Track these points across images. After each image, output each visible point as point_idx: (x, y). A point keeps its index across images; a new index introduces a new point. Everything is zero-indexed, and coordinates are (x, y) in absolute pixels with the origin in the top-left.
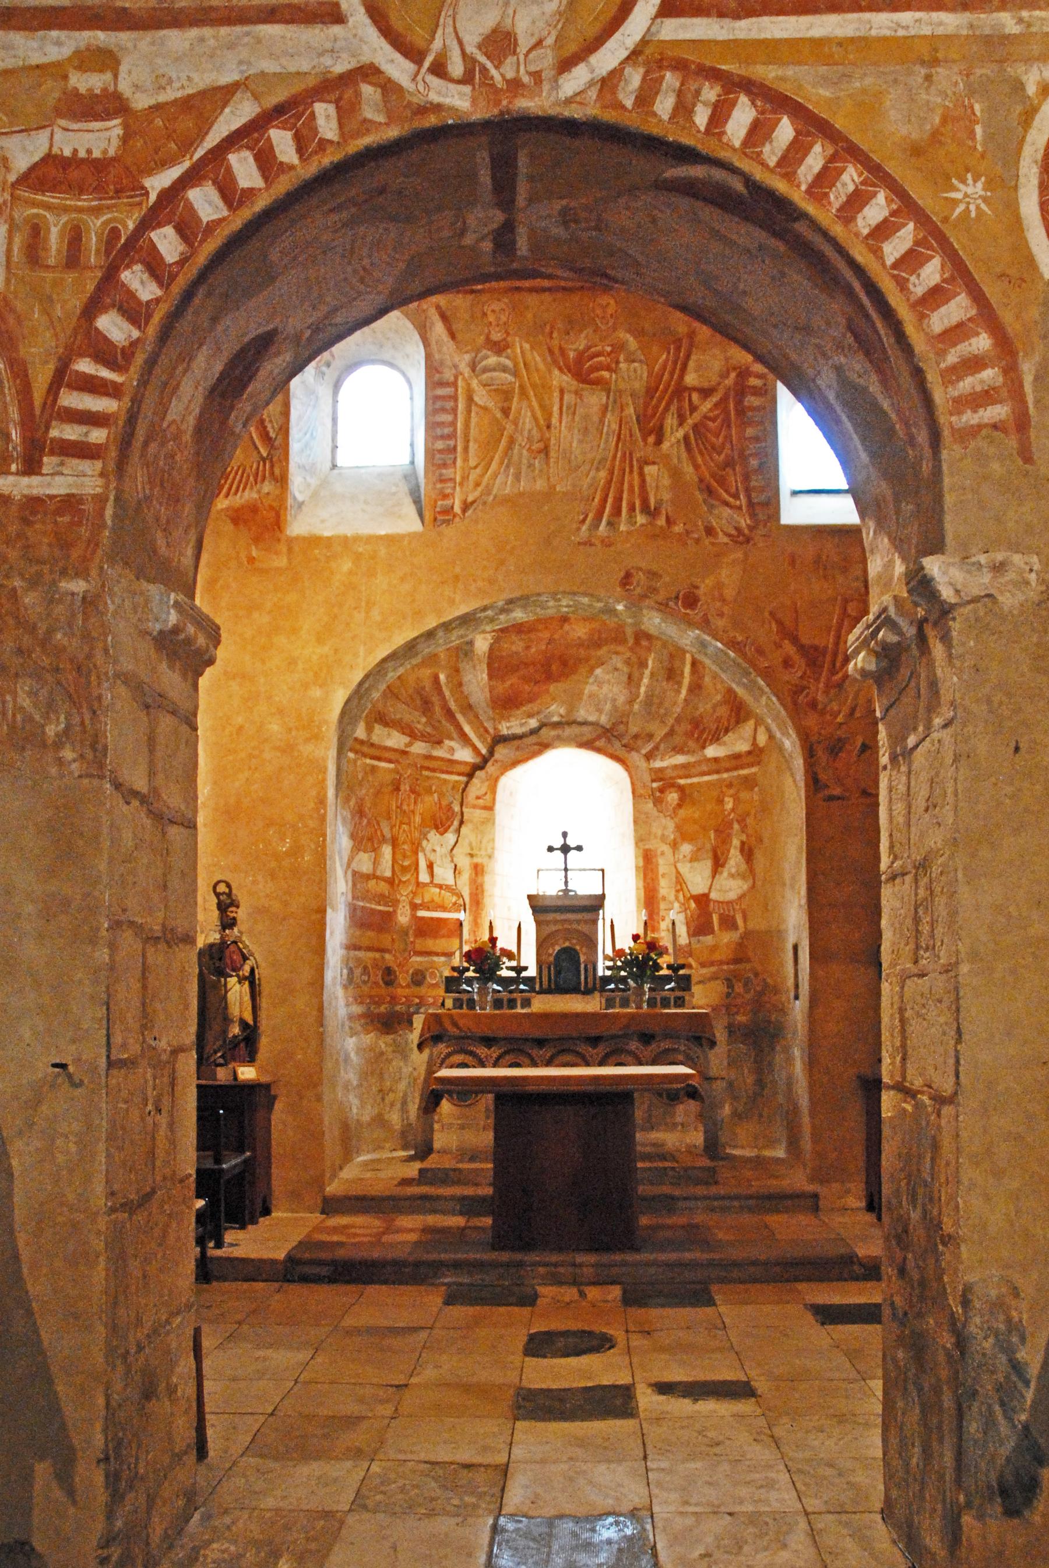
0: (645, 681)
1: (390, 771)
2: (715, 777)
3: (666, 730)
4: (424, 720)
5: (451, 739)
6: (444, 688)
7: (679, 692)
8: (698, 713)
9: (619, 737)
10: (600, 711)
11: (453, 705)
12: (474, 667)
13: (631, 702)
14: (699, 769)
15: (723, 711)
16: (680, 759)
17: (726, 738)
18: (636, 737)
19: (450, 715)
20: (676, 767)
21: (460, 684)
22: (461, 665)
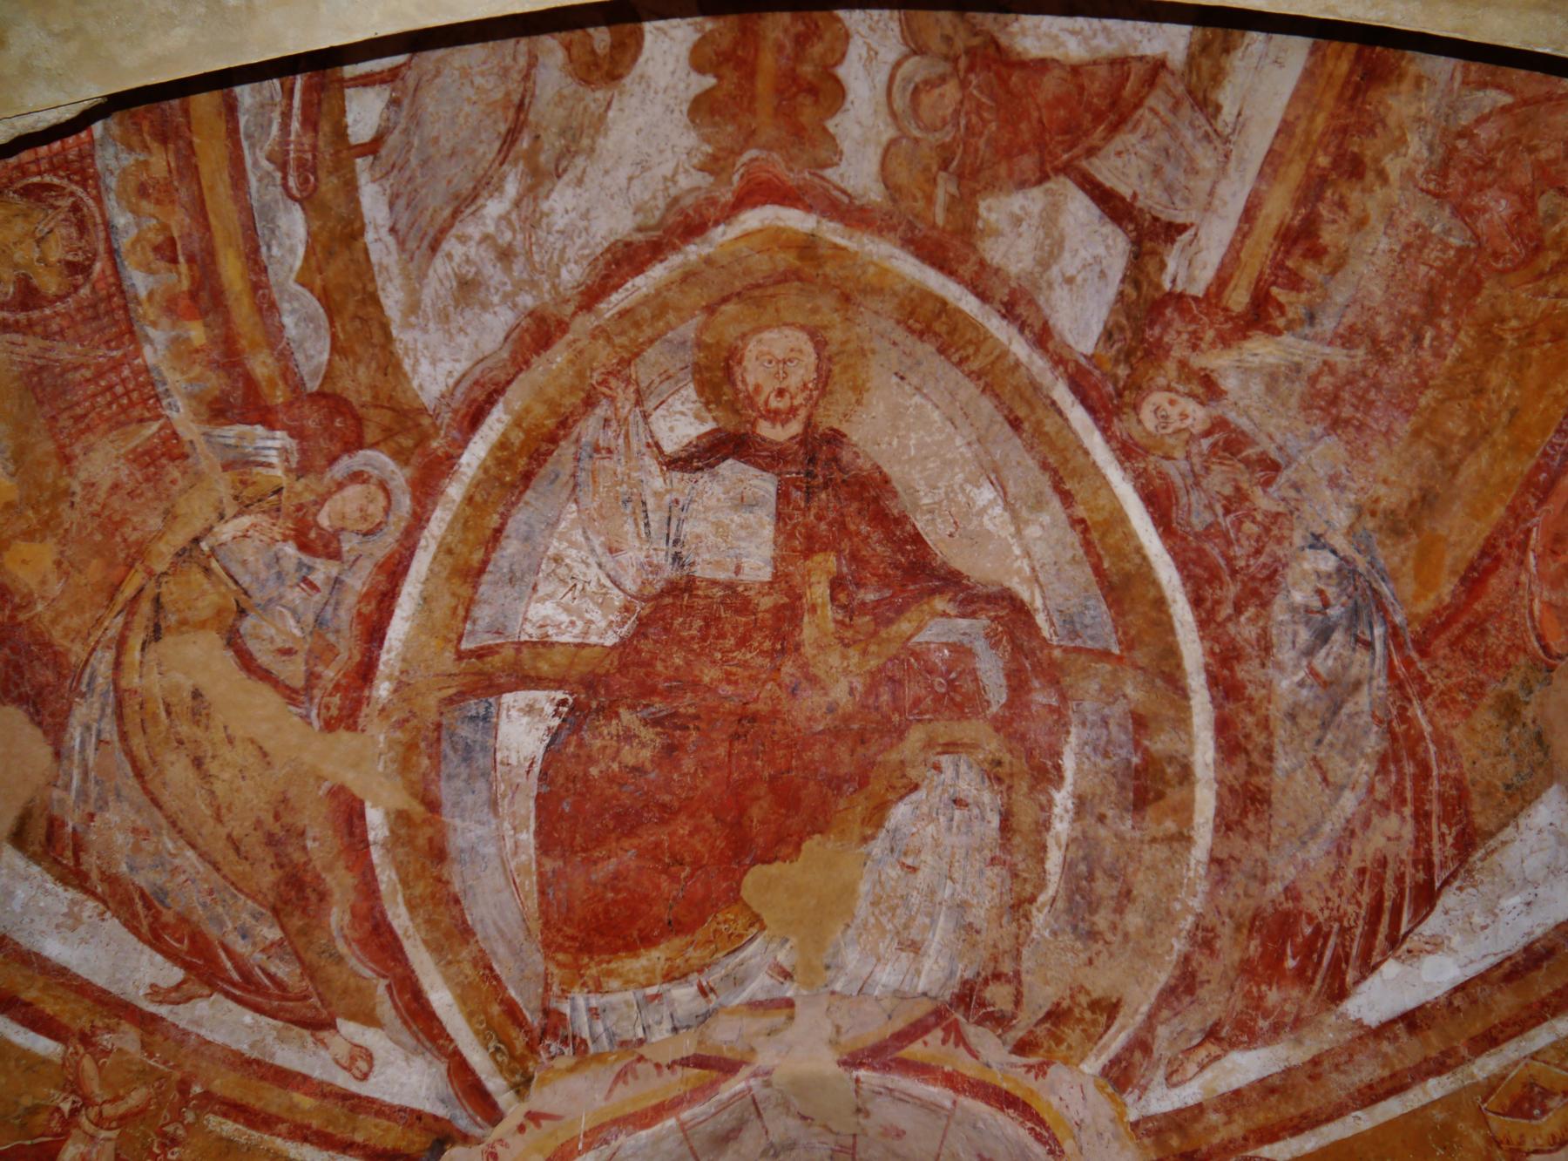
0: (1061, 827)
1: (32, 1064)
2: (1435, 1088)
3: (1163, 978)
4: (273, 934)
5: (369, 1019)
6: (376, 855)
7: (1183, 838)
8: (1275, 888)
9: (1000, 1021)
10: (915, 948)
11: (399, 918)
12: (494, 804)
13: (1020, 907)
14: (1340, 1084)
15: (1392, 833)
16: (1247, 1066)
17: (1433, 924)
18: (1057, 1016)
19: (382, 943)
20: (1235, 1099)
21: (439, 854)
22: (446, 792)
